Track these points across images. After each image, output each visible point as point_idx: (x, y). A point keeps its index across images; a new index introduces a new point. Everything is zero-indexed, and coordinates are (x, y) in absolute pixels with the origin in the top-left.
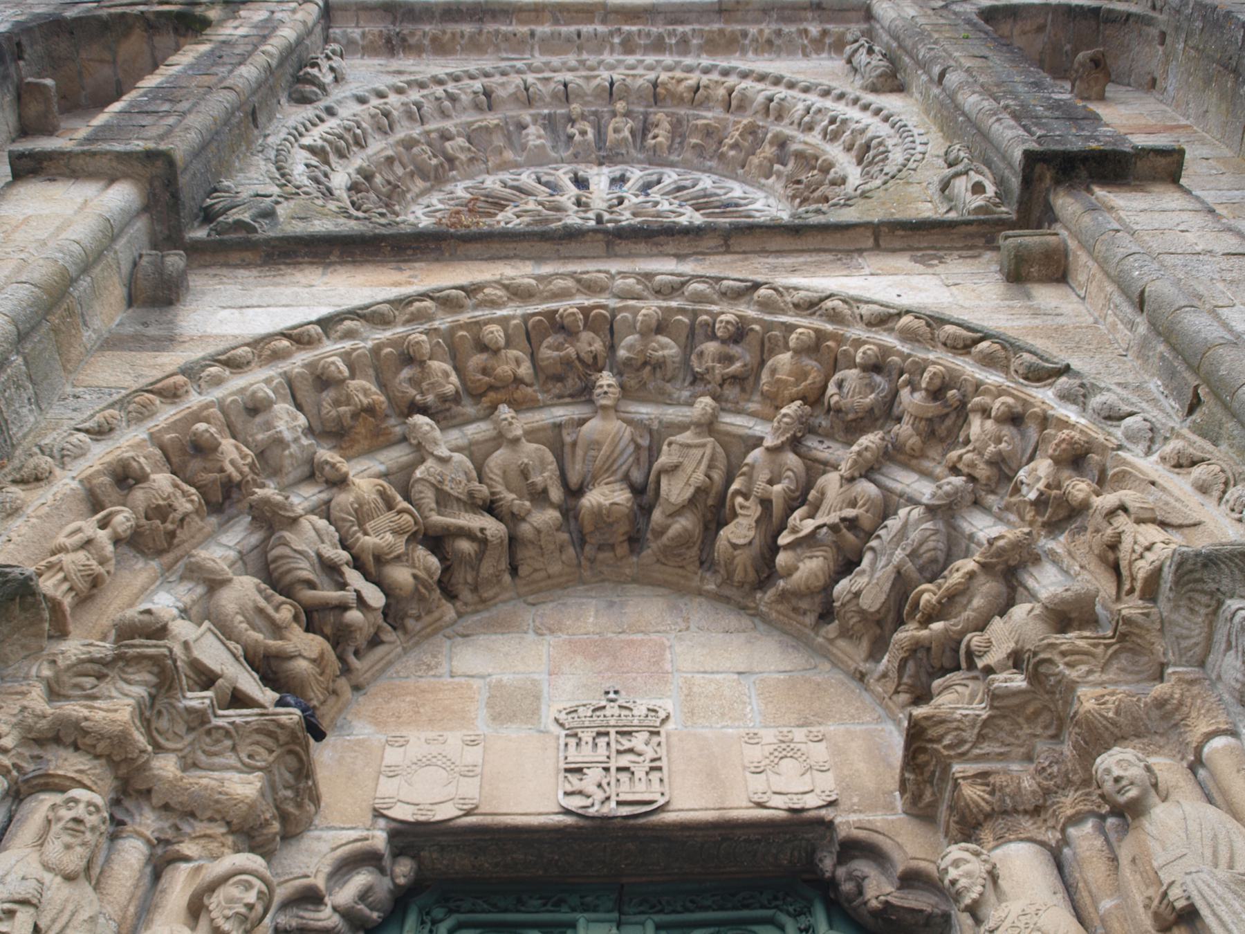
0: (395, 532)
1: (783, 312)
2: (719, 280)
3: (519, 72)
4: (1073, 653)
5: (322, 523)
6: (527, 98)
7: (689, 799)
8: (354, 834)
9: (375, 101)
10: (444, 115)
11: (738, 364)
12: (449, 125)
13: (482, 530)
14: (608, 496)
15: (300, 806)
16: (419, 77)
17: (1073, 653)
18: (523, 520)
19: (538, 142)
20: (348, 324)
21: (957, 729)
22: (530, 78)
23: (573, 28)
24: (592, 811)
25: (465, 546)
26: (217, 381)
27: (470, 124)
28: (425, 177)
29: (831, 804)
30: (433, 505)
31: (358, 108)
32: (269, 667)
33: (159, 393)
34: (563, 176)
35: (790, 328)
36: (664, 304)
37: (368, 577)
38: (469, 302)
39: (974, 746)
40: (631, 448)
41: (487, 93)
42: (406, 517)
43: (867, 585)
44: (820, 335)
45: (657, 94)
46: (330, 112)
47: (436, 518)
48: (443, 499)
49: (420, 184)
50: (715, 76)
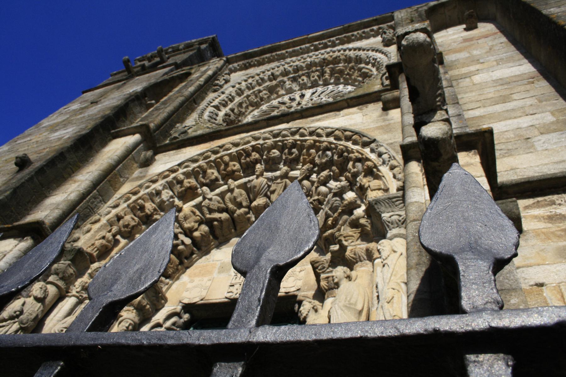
0: (196, 222)
1: (306, 136)
2: (290, 129)
3: (283, 65)
4: (347, 236)
6: (285, 73)
8: (173, 308)
9: (237, 86)
10: (260, 85)
11: (294, 155)
12: (261, 88)
13: (220, 218)
15: (158, 301)
16: (252, 75)
17: (347, 236)
18: (235, 213)
19: (289, 86)
20: (186, 164)
21: (322, 264)
22: (286, 66)
23: (298, 48)
24: (232, 297)
25: (216, 223)
26: (148, 187)
27: (268, 86)
28: (253, 106)
29: (298, 290)
30: (208, 212)
31: (231, 89)
33: (131, 193)
36: (275, 140)
37: (186, 236)
38: (221, 150)
39: (328, 268)
40: (266, 186)
41: (272, 74)
42: (198, 217)
44: (315, 141)
45: (325, 63)
46: (223, 93)
47: (208, 216)
48: (211, 211)
49: (251, 108)
50: (342, 52)
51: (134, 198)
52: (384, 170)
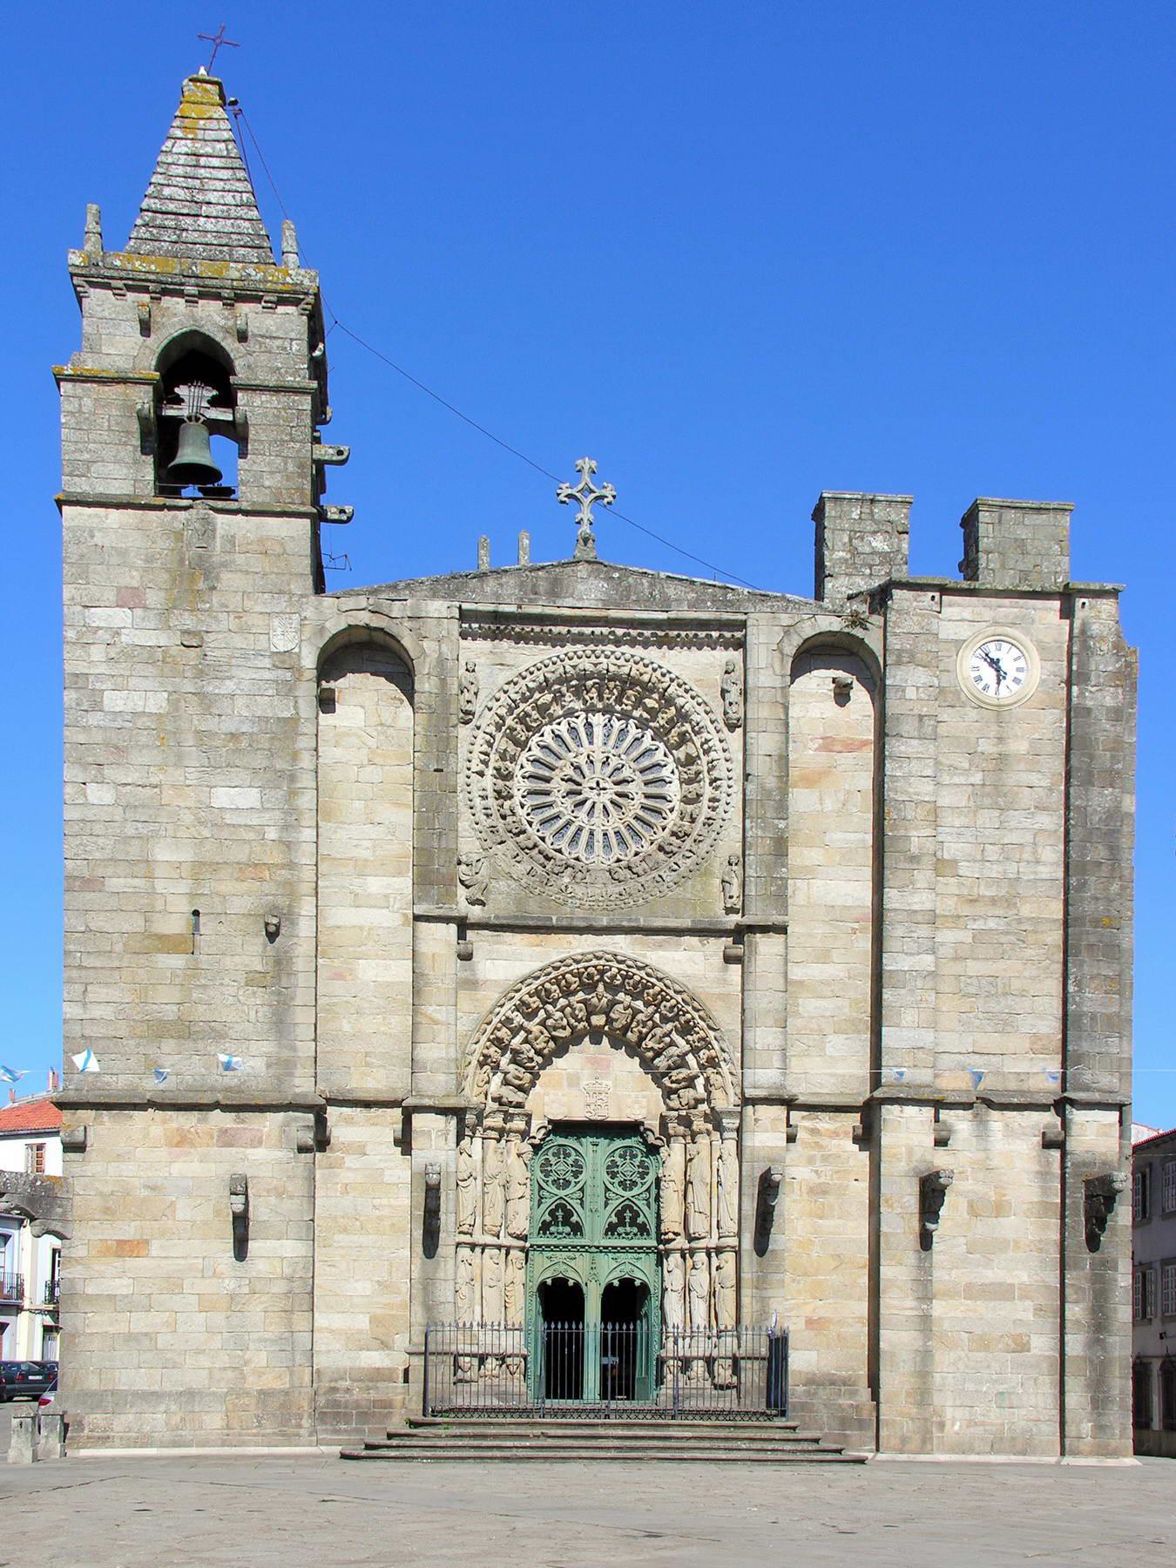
5: (527, 1046)
14: (598, 1020)
34: (580, 724)
35: (654, 985)
43: (661, 1063)
50: (658, 673)
51: (490, 1028)
52: (725, 1068)
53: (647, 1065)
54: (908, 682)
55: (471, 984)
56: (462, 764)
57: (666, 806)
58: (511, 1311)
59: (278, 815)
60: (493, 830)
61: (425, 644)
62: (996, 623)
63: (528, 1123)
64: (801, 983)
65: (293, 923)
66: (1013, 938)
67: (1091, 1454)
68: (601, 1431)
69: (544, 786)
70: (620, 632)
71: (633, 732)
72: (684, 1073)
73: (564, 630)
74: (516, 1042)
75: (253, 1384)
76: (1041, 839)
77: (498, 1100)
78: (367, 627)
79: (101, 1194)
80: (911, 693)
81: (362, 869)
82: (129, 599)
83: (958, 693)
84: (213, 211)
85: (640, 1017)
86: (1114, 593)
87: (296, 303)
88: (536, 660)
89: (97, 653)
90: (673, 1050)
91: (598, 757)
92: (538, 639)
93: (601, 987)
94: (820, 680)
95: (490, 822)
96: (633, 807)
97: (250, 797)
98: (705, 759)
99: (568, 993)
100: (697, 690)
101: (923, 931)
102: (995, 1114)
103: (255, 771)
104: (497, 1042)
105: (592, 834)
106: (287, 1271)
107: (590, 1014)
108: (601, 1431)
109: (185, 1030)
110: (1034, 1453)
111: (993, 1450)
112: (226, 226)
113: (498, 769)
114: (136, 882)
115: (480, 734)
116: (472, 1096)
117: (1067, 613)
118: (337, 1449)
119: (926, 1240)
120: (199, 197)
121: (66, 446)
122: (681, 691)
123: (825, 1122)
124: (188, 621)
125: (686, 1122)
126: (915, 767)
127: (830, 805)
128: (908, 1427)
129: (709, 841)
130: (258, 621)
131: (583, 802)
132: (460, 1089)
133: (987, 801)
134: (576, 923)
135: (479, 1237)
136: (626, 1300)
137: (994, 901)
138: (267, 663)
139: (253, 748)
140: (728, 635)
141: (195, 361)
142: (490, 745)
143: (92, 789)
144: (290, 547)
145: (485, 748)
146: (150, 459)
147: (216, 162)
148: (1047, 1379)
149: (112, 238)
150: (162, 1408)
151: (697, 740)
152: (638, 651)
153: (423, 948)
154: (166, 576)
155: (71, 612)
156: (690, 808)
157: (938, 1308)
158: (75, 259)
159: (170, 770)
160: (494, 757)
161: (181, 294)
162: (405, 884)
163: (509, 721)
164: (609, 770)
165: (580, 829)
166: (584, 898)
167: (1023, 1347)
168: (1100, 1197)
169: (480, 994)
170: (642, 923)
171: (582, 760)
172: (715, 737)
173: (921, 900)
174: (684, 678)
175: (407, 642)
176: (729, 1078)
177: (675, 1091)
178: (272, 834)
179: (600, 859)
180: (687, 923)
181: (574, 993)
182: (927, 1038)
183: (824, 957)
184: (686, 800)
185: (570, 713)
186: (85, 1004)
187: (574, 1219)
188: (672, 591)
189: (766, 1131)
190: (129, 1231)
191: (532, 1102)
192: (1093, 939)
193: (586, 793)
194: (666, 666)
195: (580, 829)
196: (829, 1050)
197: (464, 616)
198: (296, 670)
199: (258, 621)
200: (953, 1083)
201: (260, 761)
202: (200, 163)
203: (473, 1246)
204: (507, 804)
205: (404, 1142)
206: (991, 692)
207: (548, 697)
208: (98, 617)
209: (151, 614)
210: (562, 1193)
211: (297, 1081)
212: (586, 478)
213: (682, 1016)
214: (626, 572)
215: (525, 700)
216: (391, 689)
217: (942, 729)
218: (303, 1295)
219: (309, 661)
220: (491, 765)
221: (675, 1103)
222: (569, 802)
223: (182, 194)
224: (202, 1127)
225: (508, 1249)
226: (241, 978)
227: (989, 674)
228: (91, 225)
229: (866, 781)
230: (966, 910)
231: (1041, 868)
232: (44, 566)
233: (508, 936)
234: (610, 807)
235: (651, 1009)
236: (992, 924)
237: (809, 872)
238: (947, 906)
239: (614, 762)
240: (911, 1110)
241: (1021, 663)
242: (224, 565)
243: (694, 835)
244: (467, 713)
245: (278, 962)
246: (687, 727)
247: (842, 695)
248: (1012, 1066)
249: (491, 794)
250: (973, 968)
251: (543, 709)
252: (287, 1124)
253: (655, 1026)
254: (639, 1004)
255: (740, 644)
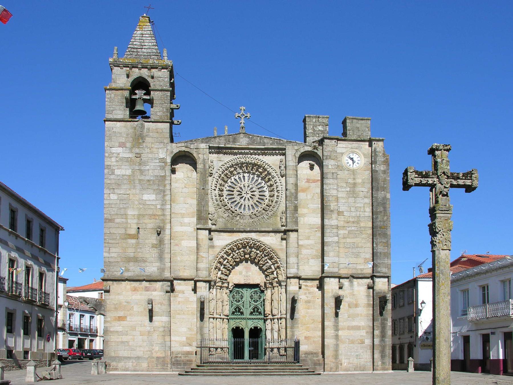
7: (252, 282)
14: (247, 256)
32: (226, 275)
34: (241, 176)
51: (218, 259)
52: (282, 269)
53: (261, 269)
54: (329, 164)
55: (213, 247)
56: (210, 187)
57: (265, 198)
58: (224, 336)
59: (160, 202)
60: (218, 205)
61: (200, 155)
62: (352, 148)
63: (228, 285)
64: (302, 245)
65: (164, 231)
66: (359, 232)
67: (380, 370)
68: (249, 368)
69: (232, 193)
70: (252, 151)
71: (256, 178)
72: (271, 270)
73: (237, 151)
74: (225, 263)
75: (155, 355)
76: (365, 206)
77: (220, 278)
78: (184, 151)
79: (114, 304)
80: (330, 167)
81: (183, 216)
82: (122, 145)
83: (342, 167)
84: (146, 47)
85: (258, 255)
86: (382, 140)
87: (167, 69)
88: (229, 159)
89: (113, 159)
90: (267, 264)
91: (246, 185)
92: (230, 154)
93: (248, 247)
94: (306, 164)
95: (217, 203)
96: (256, 198)
97: (153, 197)
98: (275, 185)
99: (239, 249)
100: (273, 167)
101: (335, 231)
102: (355, 280)
103: (154, 190)
104: (220, 262)
105: (245, 206)
106: (163, 325)
107: (245, 255)
108: (249, 368)
109: (135, 260)
110: (366, 370)
111: (355, 370)
112: (149, 51)
113: (219, 189)
114: (123, 220)
115: (214, 179)
116: (213, 277)
117: (370, 145)
118: (178, 373)
119: (337, 315)
120: (143, 44)
121: (107, 107)
122: (268, 167)
123: (309, 283)
124: (137, 151)
125: (271, 284)
126: (331, 186)
127: (309, 197)
128: (332, 365)
129: (277, 207)
130: (155, 150)
131: (242, 197)
132: (210, 275)
133: (351, 195)
134: (241, 230)
135: (215, 316)
136: (256, 333)
137: (353, 222)
138: (158, 161)
139: (154, 184)
140: (281, 152)
141: (140, 84)
142: (217, 182)
143: (111, 195)
144: (164, 130)
145: (216, 183)
146: (128, 109)
147: (147, 36)
148: (369, 351)
149: (121, 54)
150: (131, 361)
151: (273, 180)
152: (257, 156)
153: (200, 237)
154: (131, 139)
155: (107, 149)
156: (271, 198)
157: (340, 333)
158: (111, 60)
159: (132, 190)
160: (218, 185)
161: (137, 67)
162: (194, 220)
163: (222, 176)
164: (249, 188)
165: (242, 204)
166: (242, 223)
167: (363, 342)
168: (383, 301)
169: (215, 250)
170: (259, 229)
171: (242, 186)
172: (278, 179)
173: (334, 222)
174: (269, 163)
175: (195, 155)
176: (283, 272)
177: (268, 275)
178: (159, 207)
179: (247, 212)
180: (271, 229)
181: (241, 249)
182: (336, 259)
183: (308, 238)
184: (270, 196)
185: (239, 173)
186: (109, 253)
187: (241, 311)
188: (266, 141)
189: (293, 286)
190: (121, 314)
191: (229, 279)
192: (380, 232)
193: (243, 195)
194: (264, 160)
195: (242, 204)
196: (310, 264)
197: (210, 148)
198: (165, 163)
199: (155, 150)
200: (343, 272)
201: (156, 187)
202: (144, 37)
203: (214, 318)
204: (222, 198)
205: (195, 290)
206: (351, 166)
207: (233, 169)
208: (114, 150)
209: (127, 149)
210: (238, 304)
211: (166, 273)
212: (243, 111)
213: (269, 254)
214: (253, 136)
215: (226, 170)
216: (191, 168)
217: (338, 176)
218: (168, 331)
219: (169, 160)
220: (218, 187)
221: (268, 279)
222: (239, 197)
223: (138, 43)
224: (140, 286)
225: (223, 319)
226: (151, 246)
227: (351, 162)
228: (115, 52)
229: (319, 190)
230: (346, 225)
231: (366, 213)
232: (100, 137)
233: (222, 234)
234: (250, 198)
235: (262, 253)
236: (353, 228)
237: (304, 215)
238: (341, 224)
239: (251, 186)
240: (332, 279)
241: (359, 159)
242: (146, 136)
243: (273, 206)
244: (211, 173)
245: (160, 241)
246: (270, 176)
247: (312, 168)
248: (359, 267)
249: (217, 195)
250: (348, 240)
251: (231, 172)
252: (163, 285)
253: (263, 257)
254: (258, 252)
255: (284, 154)
